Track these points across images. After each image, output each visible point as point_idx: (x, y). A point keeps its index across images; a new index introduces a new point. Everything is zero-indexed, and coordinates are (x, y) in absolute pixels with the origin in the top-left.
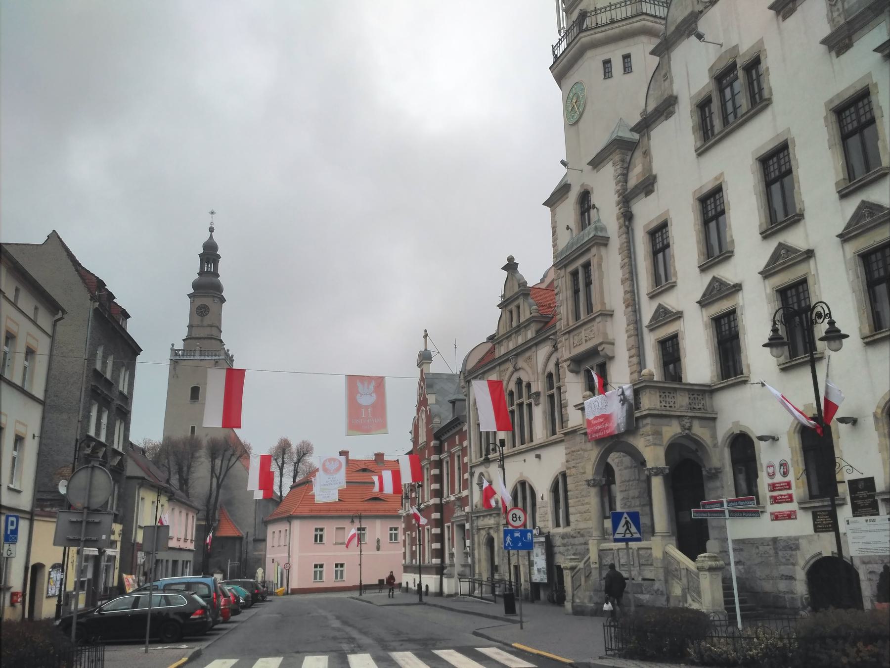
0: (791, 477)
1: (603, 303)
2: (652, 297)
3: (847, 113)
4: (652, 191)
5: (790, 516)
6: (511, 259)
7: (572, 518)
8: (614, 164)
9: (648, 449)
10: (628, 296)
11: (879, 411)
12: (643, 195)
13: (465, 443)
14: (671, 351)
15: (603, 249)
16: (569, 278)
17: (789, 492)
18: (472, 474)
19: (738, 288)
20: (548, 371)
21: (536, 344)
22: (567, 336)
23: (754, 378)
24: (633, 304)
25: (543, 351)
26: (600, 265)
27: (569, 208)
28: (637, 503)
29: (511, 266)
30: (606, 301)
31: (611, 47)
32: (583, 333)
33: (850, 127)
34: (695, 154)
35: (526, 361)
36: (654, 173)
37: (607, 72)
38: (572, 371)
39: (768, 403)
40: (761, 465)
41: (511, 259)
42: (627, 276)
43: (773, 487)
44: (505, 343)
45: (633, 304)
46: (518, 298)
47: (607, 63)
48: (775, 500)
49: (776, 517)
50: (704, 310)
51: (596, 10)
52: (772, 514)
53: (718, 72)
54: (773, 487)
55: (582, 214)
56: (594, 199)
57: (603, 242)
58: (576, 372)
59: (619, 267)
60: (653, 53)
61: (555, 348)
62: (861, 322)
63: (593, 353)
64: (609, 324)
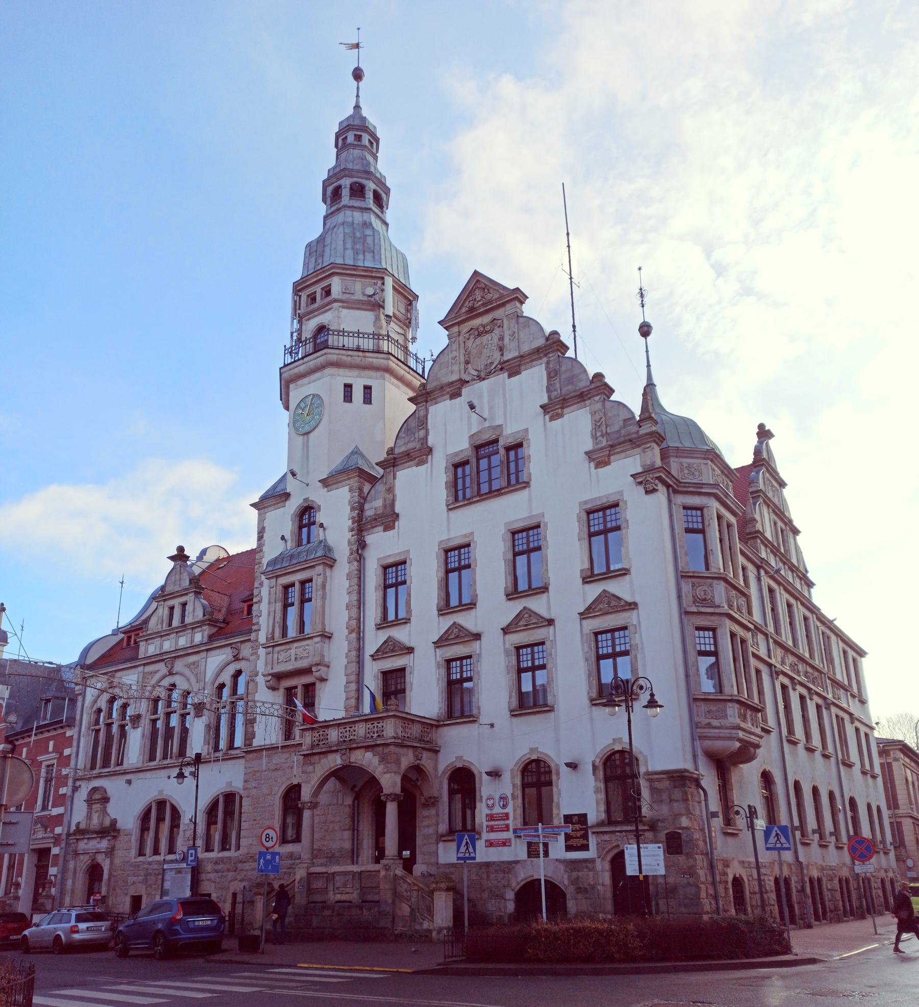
0: (509, 809)
1: (323, 624)
2: (379, 627)
3: (596, 515)
4: (393, 528)
5: (505, 843)
6: (181, 549)
7: (243, 842)
8: (350, 490)
9: (388, 776)
10: (354, 622)
11: (598, 760)
12: (381, 528)
13: (67, 752)
14: (394, 684)
15: (328, 570)
16: (280, 589)
17: (507, 822)
18: (75, 789)
19: (477, 636)
20: (220, 680)
21: (207, 650)
22: (271, 649)
23: (484, 719)
24: (358, 630)
25: (216, 660)
26: (324, 586)
27: (283, 520)
28: (337, 828)
29: (180, 557)
30: (327, 622)
31: (356, 372)
32: (294, 649)
33: (597, 528)
34: (445, 508)
35: (188, 666)
36: (397, 511)
37: (348, 398)
38: (269, 688)
39: (492, 744)
40: (481, 797)
41: (181, 549)
42: (355, 603)
43: (491, 817)
44: (157, 641)
45: (358, 630)
46: (186, 594)
47: (348, 387)
48: (491, 829)
49: (490, 844)
50: (437, 650)
51: (344, 331)
52: (486, 841)
53: (479, 442)
54: (491, 817)
55: (301, 528)
56: (320, 517)
57: (329, 561)
58: (273, 689)
59: (345, 592)
60: (410, 400)
61: (236, 658)
62: (590, 687)
63: (307, 671)
64: (326, 646)
